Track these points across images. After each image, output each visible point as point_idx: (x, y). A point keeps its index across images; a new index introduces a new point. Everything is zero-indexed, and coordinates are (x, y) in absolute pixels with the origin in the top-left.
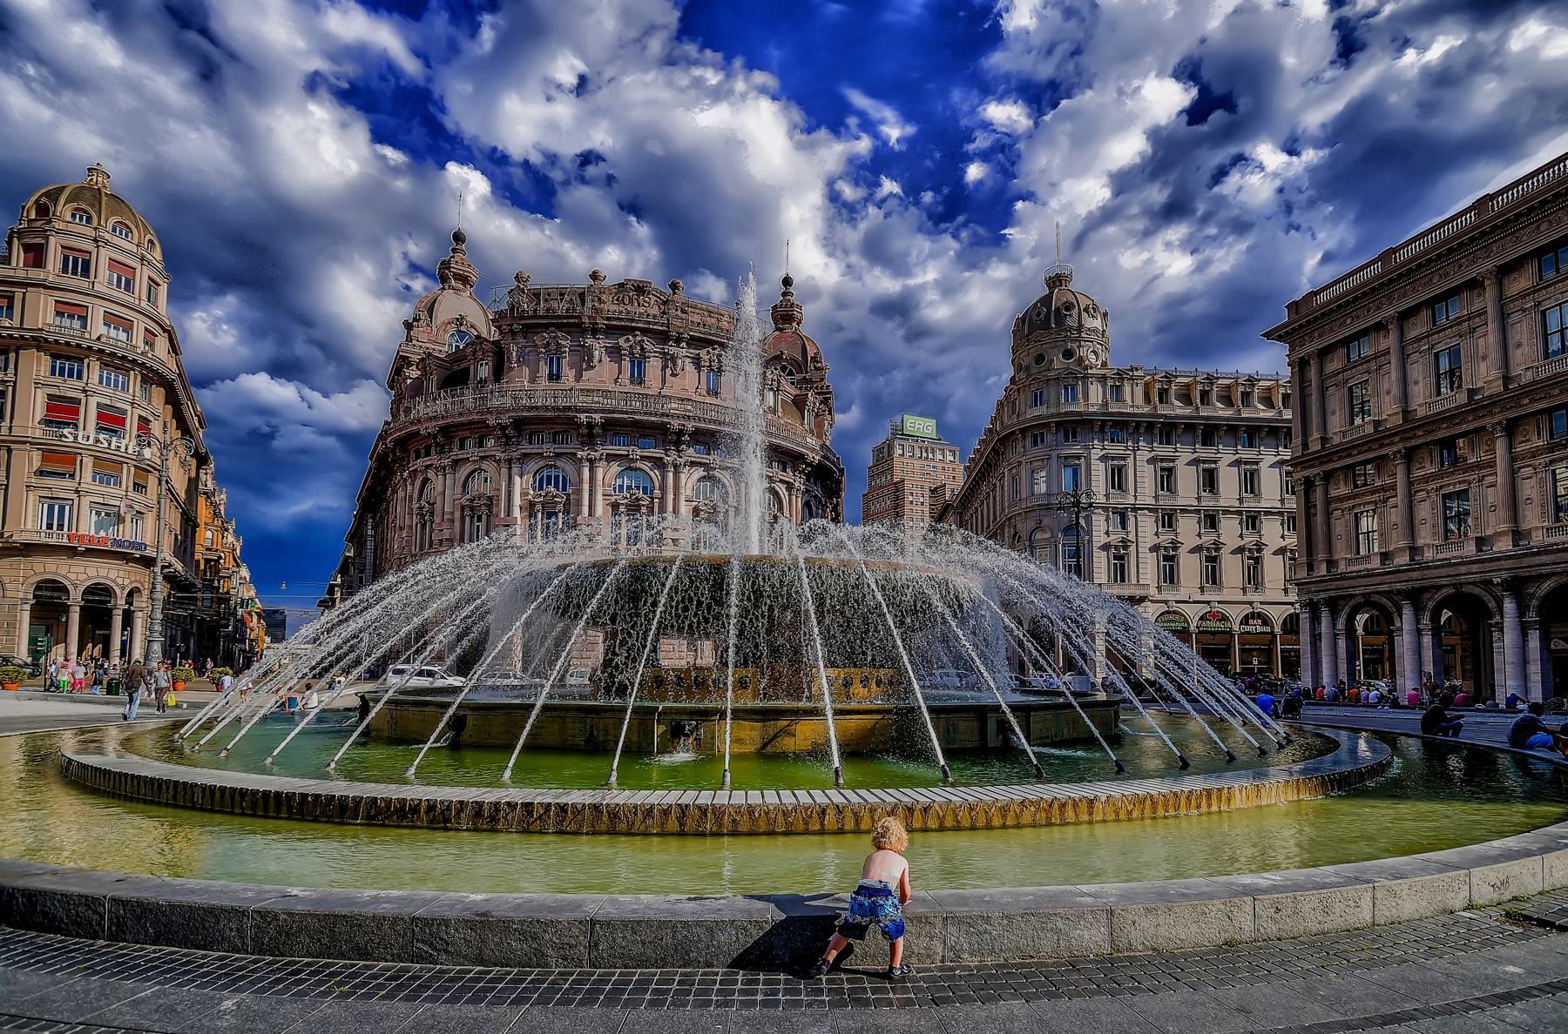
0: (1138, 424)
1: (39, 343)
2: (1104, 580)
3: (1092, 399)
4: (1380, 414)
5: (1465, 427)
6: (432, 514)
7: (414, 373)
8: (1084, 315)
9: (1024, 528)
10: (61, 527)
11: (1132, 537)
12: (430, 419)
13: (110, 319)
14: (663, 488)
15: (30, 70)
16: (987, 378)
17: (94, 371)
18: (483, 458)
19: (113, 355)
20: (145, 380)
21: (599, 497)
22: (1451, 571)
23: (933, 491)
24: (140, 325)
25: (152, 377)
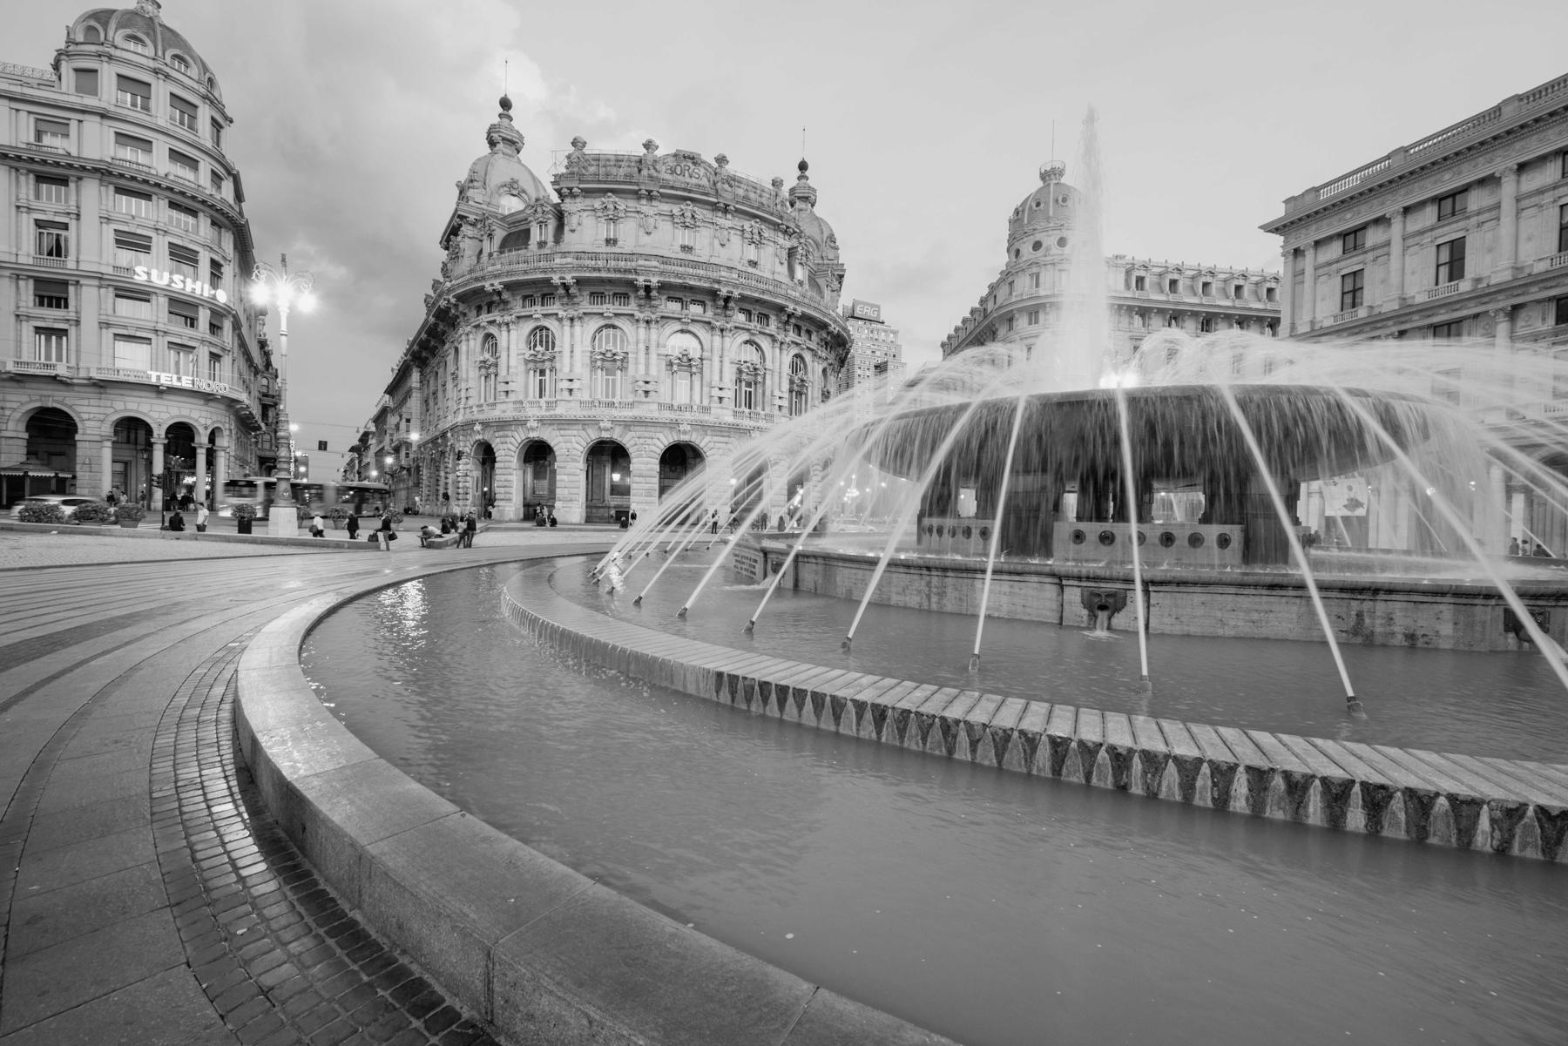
18: (545, 316)
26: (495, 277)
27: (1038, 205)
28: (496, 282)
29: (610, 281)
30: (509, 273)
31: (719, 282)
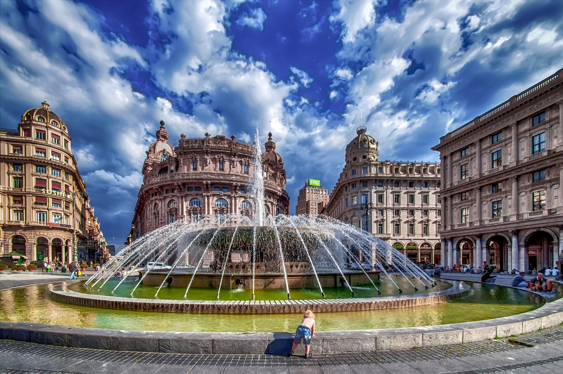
0: (388, 180)
1: (32, 161)
2: (375, 232)
3: (372, 172)
4: (471, 175)
5: (501, 179)
6: (158, 214)
7: (150, 169)
8: (370, 143)
9: (349, 216)
10: (44, 220)
11: (385, 218)
12: (156, 184)
13: (53, 153)
14: (231, 204)
15: (19, 69)
16: (337, 166)
17: (50, 171)
19: (55, 165)
20: (67, 174)
21: (211, 208)
22: (494, 228)
23: (319, 204)
24: (63, 155)
25: (68, 172)
26: (156, 184)
27: (355, 144)
28: (156, 186)
29: (194, 183)
30: (160, 183)
31: (232, 181)
